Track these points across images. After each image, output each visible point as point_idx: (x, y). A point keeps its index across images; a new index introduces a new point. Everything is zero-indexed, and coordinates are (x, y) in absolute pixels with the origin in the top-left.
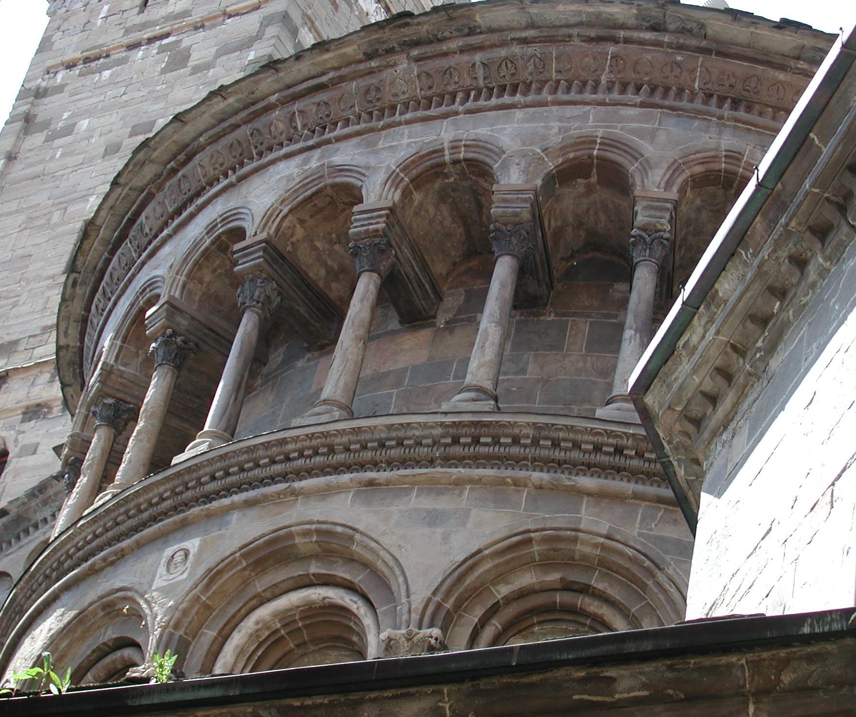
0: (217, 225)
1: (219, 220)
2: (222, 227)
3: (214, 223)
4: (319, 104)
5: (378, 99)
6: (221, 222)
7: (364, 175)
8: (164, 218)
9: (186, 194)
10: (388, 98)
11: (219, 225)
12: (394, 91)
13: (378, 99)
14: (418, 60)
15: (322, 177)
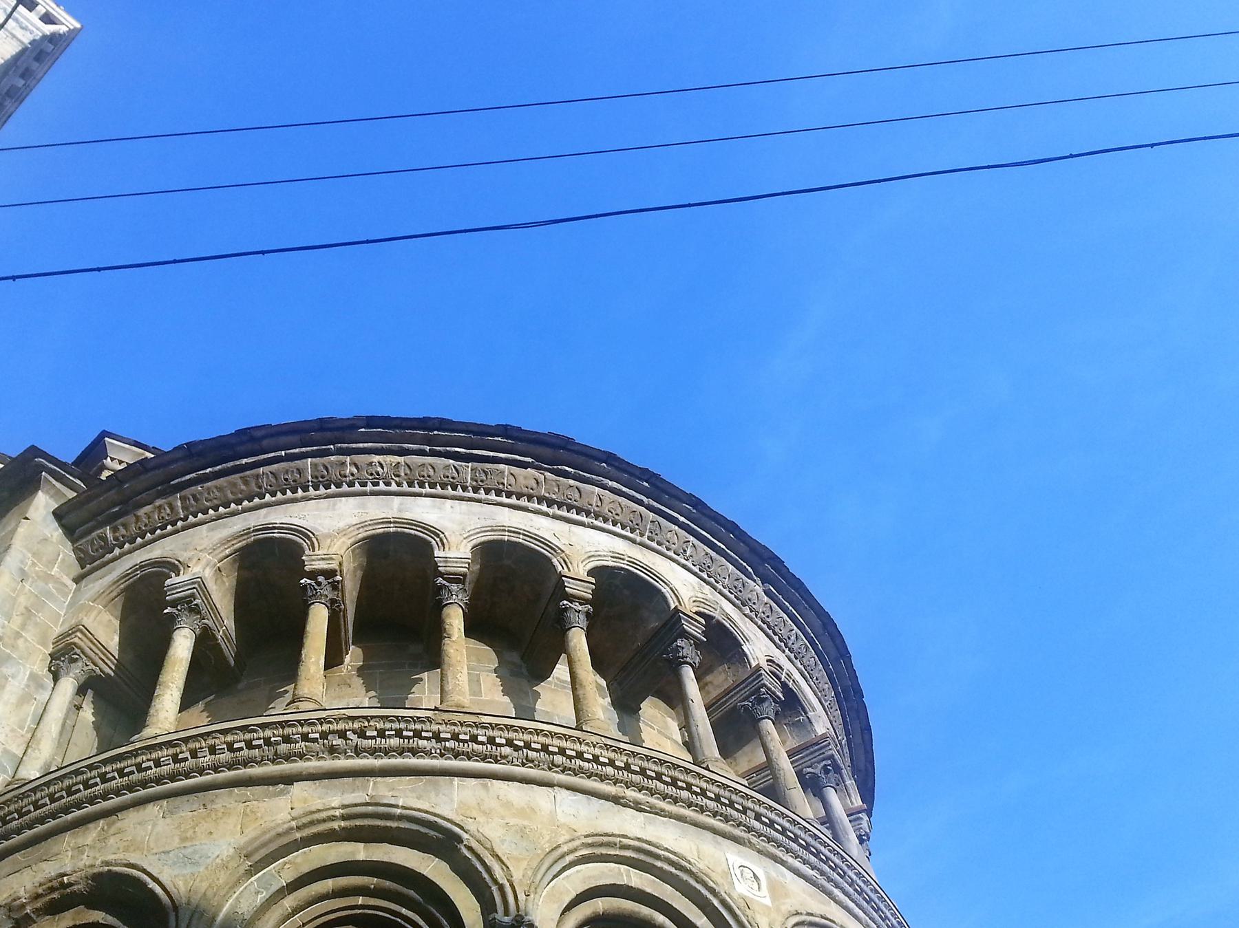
0: (623, 559)
1: (628, 559)
2: (628, 565)
3: (622, 557)
4: (707, 554)
5: (740, 591)
6: (628, 561)
7: (748, 640)
8: (531, 491)
9: (571, 499)
10: (745, 595)
11: (625, 562)
12: (750, 596)
13: (740, 591)
14: (767, 593)
15: (716, 610)
